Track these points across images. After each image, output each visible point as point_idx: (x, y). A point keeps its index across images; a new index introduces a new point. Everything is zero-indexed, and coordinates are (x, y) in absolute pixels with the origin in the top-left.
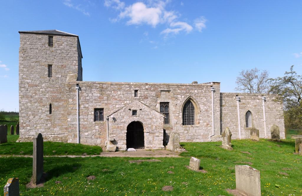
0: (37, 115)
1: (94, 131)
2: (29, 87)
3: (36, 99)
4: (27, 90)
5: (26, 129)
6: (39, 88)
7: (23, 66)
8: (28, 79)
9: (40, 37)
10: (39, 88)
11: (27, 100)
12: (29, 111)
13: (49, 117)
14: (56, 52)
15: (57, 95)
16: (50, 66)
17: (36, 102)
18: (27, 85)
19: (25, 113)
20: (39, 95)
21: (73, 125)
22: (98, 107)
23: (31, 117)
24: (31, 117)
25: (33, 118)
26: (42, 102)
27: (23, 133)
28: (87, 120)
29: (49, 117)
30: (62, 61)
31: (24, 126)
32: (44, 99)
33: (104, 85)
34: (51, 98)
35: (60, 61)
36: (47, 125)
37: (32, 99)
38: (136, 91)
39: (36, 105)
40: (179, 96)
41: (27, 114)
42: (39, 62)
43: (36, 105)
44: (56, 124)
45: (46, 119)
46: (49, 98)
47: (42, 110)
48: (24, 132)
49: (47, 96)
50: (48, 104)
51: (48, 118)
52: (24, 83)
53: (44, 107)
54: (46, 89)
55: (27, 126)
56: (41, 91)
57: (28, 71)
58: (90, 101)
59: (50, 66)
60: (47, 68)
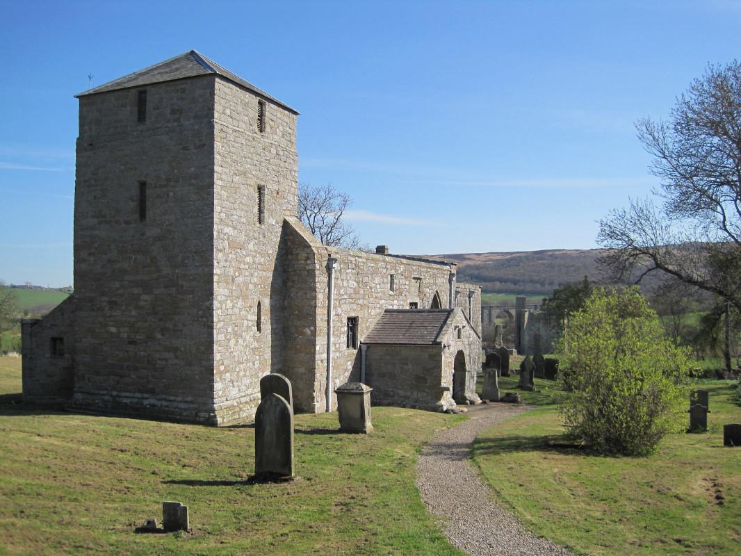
4: (226, 261)
8: (228, 225)
16: (260, 189)
17: (238, 298)
19: (222, 330)
20: (245, 276)
22: (353, 315)
23: (233, 342)
29: (257, 342)
30: (276, 179)
32: (251, 287)
37: (234, 288)
38: (392, 276)
39: (239, 305)
40: (428, 290)
43: (239, 305)
45: (253, 347)
47: (247, 320)
51: (256, 344)
56: (248, 263)
58: (344, 299)
59: (260, 189)
60: (257, 195)
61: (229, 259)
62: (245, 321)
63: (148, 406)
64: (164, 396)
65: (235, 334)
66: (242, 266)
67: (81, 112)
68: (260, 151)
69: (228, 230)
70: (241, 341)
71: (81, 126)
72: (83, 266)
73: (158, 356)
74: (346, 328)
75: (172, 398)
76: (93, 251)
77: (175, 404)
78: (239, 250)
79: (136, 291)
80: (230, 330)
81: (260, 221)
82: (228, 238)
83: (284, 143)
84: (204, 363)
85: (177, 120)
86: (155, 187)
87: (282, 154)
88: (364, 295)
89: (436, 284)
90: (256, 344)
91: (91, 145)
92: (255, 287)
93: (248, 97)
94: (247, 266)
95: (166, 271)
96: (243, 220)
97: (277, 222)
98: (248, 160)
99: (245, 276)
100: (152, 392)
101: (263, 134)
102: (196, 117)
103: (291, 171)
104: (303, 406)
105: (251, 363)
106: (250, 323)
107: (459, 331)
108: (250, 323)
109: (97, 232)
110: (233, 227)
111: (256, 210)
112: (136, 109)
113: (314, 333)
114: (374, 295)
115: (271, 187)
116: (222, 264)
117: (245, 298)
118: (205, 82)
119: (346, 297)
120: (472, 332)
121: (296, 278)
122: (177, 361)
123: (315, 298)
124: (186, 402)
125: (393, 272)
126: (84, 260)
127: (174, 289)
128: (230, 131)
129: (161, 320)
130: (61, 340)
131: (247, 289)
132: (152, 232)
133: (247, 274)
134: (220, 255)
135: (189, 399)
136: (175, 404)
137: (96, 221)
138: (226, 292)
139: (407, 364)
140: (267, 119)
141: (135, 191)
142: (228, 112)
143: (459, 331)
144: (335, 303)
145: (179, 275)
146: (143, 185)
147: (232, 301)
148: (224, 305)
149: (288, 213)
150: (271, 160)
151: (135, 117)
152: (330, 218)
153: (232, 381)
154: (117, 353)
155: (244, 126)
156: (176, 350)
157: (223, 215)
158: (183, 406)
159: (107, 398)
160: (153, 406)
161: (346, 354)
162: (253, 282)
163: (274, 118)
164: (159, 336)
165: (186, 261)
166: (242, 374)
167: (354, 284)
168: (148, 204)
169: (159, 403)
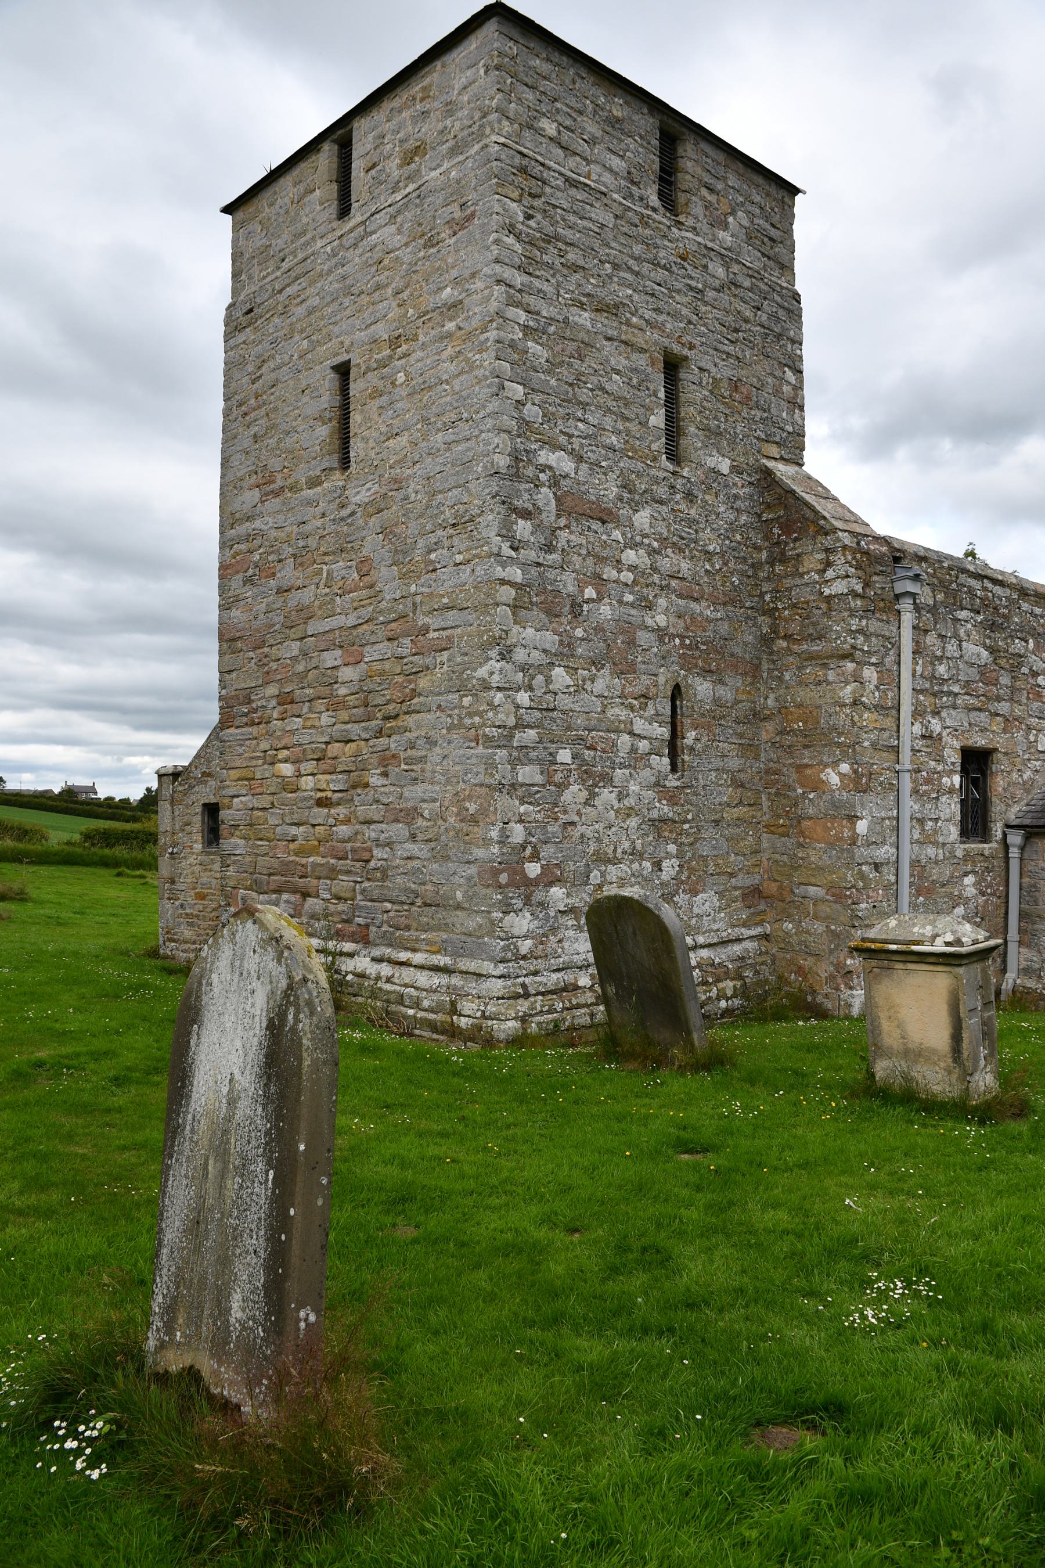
0: (607, 779)
2: (562, 522)
3: (598, 629)
4: (549, 548)
5: (543, 905)
6: (617, 535)
8: (555, 447)
9: (618, 113)
10: (617, 535)
11: (550, 639)
13: (672, 797)
14: (705, 267)
15: (709, 620)
16: (672, 366)
17: (596, 663)
18: (546, 496)
19: (533, 754)
20: (620, 602)
21: (877, 866)
22: (980, 741)
23: (575, 794)
24: (575, 794)
25: (587, 803)
26: (632, 668)
27: (525, 946)
28: (935, 832)
29: (672, 801)
30: (730, 349)
31: (529, 883)
32: (644, 638)
33: (998, 590)
34: (682, 637)
36: (658, 865)
37: (579, 633)
39: (599, 686)
44: (704, 859)
45: (655, 814)
46: (673, 637)
47: (631, 733)
48: (526, 937)
49: (661, 620)
50: (664, 678)
51: (665, 809)
52: (530, 471)
53: (644, 707)
54: (657, 552)
55: (549, 879)
56: (632, 568)
57: (553, 366)
58: (949, 693)
59: (672, 366)
61: (561, 543)
62: (625, 738)
63: (349, 977)
64: (388, 951)
67: (235, 242)
70: (607, 795)
72: (235, 613)
73: (373, 835)
74: (957, 779)
75: (403, 956)
76: (251, 572)
77: (407, 974)
78: (596, 525)
79: (331, 658)
80: (565, 756)
81: (674, 455)
82: (555, 483)
83: (751, 258)
84: (479, 853)
86: (369, 369)
87: (747, 283)
88: (1013, 690)
90: (665, 809)
91: (251, 311)
92: (661, 640)
93: (618, 107)
94: (627, 577)
95: (390, 591)
97: (736, 470)
98: (629, 276)
99: (620, 602)
100: (363, 938)
101: (681, 218)
102: (453, 152)
103: (779, 336)
104: (820, 999)
105: (647, 865)
106: (643, 745)
110: (571, 453)
111: (657, 420)
112: (335, 186)
117: (625, 669)
118: (474, 46)
119: (956, 689)
121: (794, 628)
122: (413, 848)
124: (436, 969)
127: (407, 641)
129: (379, 733)
131: (631, 643)
132: (361, 495)
133: (629, 598)
134: (523, 528)
135: (443, 960)
141: (327, 398)
142: (550, 128)
144: (917, 704)
145: (418, 599)
146: (343, 371)
147: (571, 670)
148: (540, 678)
149: (774, 451)
150: (711, 294)
151: (333, 209)
153: (571, 911)
154: (293, 830)
155: (607, 178)
156: (411, 814)
157: (531, 412)
160: (362, 976)
161: (959, 853)
162: (649, 622)
163: (720, 186)
165: (433, 556)
167: (976, 651)
168: (356, 418)
169: (372, 969)
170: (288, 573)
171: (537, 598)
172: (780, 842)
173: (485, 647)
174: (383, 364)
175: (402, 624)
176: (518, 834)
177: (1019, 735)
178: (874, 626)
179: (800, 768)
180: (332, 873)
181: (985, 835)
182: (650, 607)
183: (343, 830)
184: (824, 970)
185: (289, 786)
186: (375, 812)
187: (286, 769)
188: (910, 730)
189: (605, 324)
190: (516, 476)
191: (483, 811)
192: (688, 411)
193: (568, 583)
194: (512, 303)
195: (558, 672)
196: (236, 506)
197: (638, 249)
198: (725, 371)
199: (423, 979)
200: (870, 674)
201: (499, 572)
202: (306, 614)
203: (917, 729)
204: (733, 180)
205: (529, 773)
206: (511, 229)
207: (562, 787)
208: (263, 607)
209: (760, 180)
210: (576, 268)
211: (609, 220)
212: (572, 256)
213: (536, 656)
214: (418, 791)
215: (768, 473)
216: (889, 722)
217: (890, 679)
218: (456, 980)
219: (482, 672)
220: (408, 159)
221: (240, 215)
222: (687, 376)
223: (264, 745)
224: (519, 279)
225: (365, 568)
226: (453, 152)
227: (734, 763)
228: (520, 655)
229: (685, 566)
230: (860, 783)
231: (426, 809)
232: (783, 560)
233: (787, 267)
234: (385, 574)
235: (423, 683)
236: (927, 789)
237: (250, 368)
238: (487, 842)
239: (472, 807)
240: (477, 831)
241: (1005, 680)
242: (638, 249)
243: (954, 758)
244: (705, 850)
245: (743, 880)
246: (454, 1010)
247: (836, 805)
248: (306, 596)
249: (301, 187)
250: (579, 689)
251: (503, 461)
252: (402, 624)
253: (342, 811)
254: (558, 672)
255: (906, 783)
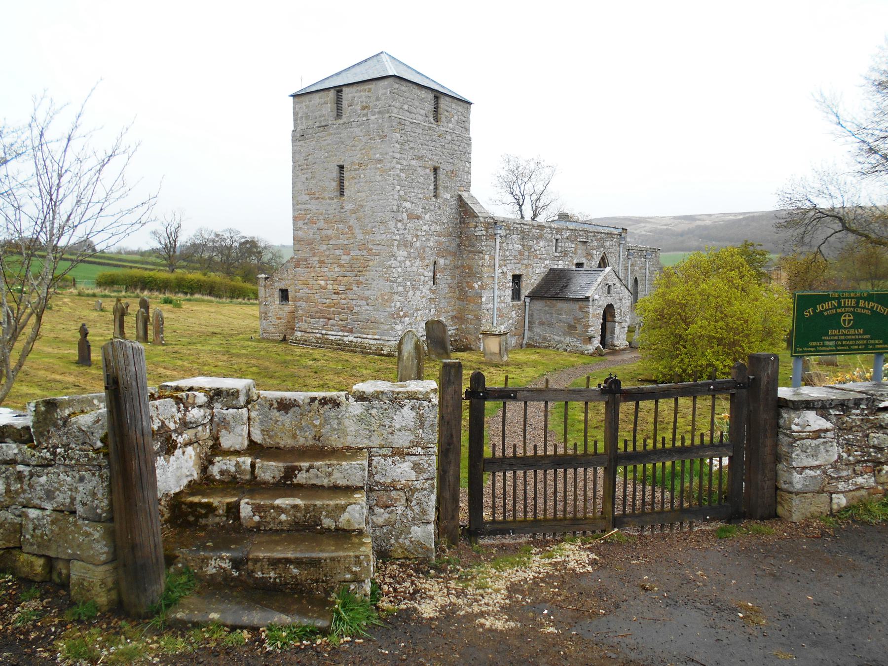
1: (511, 321)
4: (405, 229)
7: (399, 166)
8: (406, 201)
11: (405, 254)
12: (407, 280)
13: (433, 292)
16: (435, 169)
22: (518, 272)
23: (411, 293)
26: (424, 258)
29: (434, 293)
30: (451, 161)
31: (401, 317)
32: (427, 249)
35: (451, 161)
39: (417, 264)
40: (595, 252)
41: (405, 286)
42: (420, 158)
49: (432, 244)
51: (432, 296)
55: (405, 316)
59: (435, 169)
65: (415, 288)
66: (419, 233)
67: (294, 108)
68: (435, 137)
69: (408, 205)
70: (418, 293)
71: (295, 120)
75: (365, 336)
77: (366, 341)
79: (338, 252)
80: (408, 284)
81: (436, 196)
84: (388, 309)
85: (364, 115)
89: (603, 246)
90: (432, 296)
93: (423, 94)
95: (360, 237)
96: (421, 196)
97: (452, 197)
102: (379, 113)
106: (427, 279)
107: (609, 287)
108: (427, 279)
109: (309, 206)
111: (432, 187)
113: (482, 287)
114: (539, 256)
115: (445, 167)
116: (401, 232)
117: (423, 259)
120: (623, 288)
121: (467, 243)
122: (368, 308)
123: (483, 258)
125: (558, 237)
126: (300, 229)
128: (408, 123)
129: (356, 275)
130: (287, 290)
131: (424, 251)
132: (349, 206)
134: (399, 224)
135: (376, 337)
136: (366, 341)
137: (308, 197)
138: (405, 254)
139: (561, 315)
140: (440, 110)
141: (335, 173)
142: (406, 107)
143: (609, 287)
146: (341, 167)
149: (462, 189)
150: (446, 146)
152: (539, 187)
157: (402, 193)
158: (371, 342)
159: (318, 335)
163: (449, 109)
164: (354, 288)
166: (419, 318)
168: (346, 183)
170: (321, 224)
171: (405, 244)
172: (461, 303)
173: (390, 257)
174: (356, 170)
175: (363, 246)
176: (398, 304)
177: (530, 269)
178: (489, 243)
179: (467, 282)
180: (340, 314)
181: (519, 299)
182: (428, 240)
183: (343, 302)
184: (473, 338)
185: (321, 287)
186: (354, 297)
187: (323, 283)
188: (498, 271)
189: (421, 163)
190: (398, 211)
191: (390, 299)
192: (440, 183)
193: (409, 237)
194: (397, 163)
195: (407, 262)
196: (299, 198)
197: (428, 138)
198: (450, 168)
199: (371, 342)
200: (487, 257)
201: (394, 238)
202: (329, 238)
203: (500, 271)
204: (454, 106)
205: (401, 289)
206: (397, 142)
207: (408, 292)
208: (311, 233)
209: (461, 103)
210: (412, 148)
211: (420, 131)
212: (412, 145)
213: (403, 259)
214: (370, 292)
215: (460, 196)
216: (492, 270)
217: (493, 258)
218: (381, 342)
219: (389, 263)
220: (364, 108)
221: (296, 99)
222: (440, 172)
223: (313, 274)
224: (398, 156)
225: (350, 228)
226: (379, 113)
227: (449, 281)
228: (399, 259)
229: (438, 228)
230: (482, 287)
231: (372, 297)
232: (464, 223)
233: (467, 130)
234: (357, 231)
235: (371, 263)
236: (502, 288)
237: (303, 155)
238: (391, 307)
239: (386, 298)
240: (388, 304)
241: (526, 253)
242: (428, 138)
243: (510, 278)
244: (441, 306)
245: (451, 314)
246: (382, 350)
247: (477, 293)
248: (329, 232)
249: (323, 101)
250: (412, 266)
251: (395, 208)
252: (363, 246)
253: (343, 296)
254: (407, 262)
255: (496, 287)
